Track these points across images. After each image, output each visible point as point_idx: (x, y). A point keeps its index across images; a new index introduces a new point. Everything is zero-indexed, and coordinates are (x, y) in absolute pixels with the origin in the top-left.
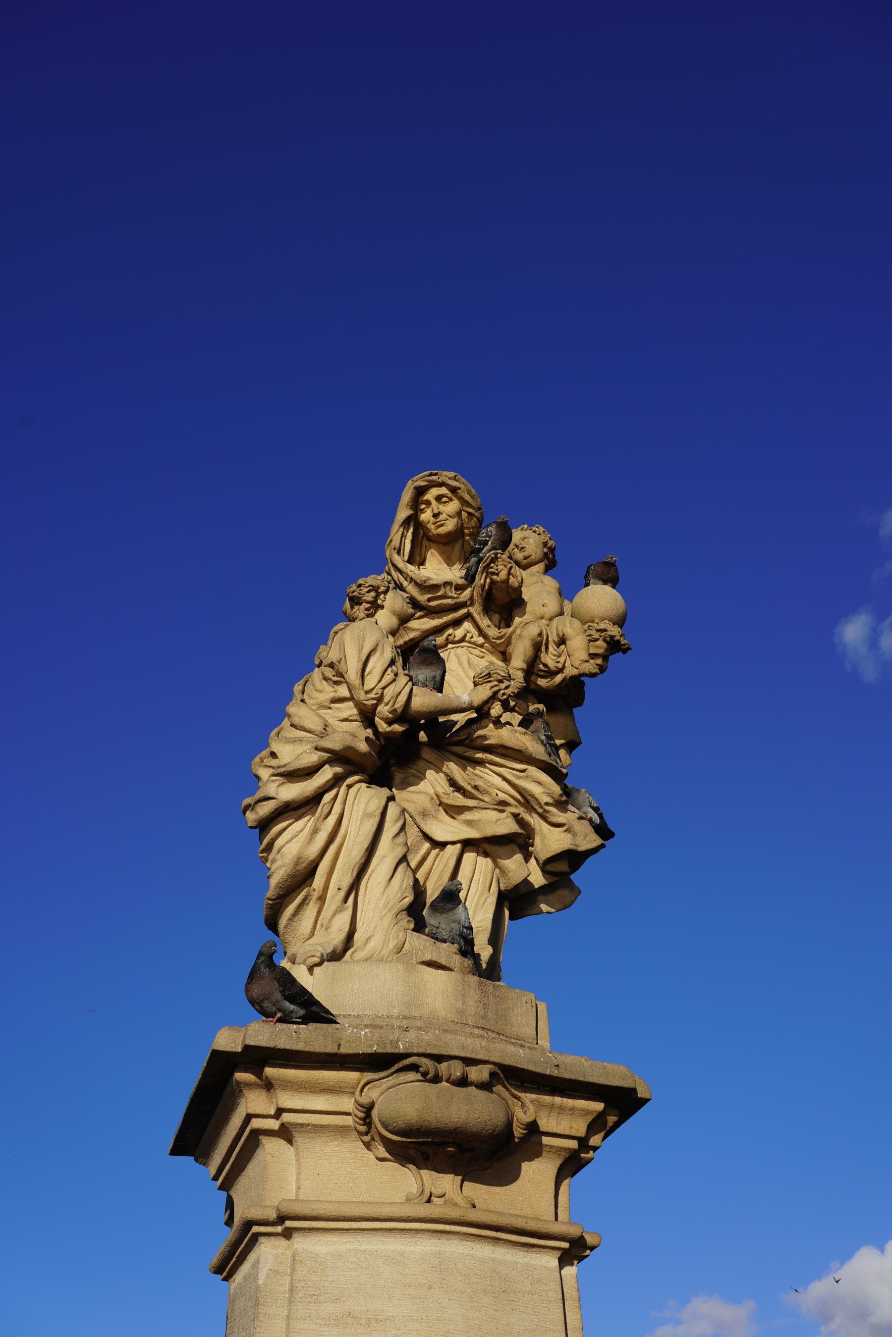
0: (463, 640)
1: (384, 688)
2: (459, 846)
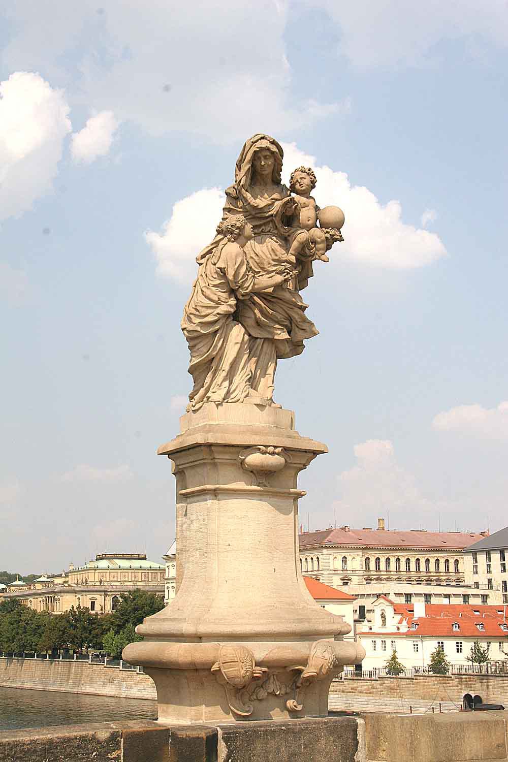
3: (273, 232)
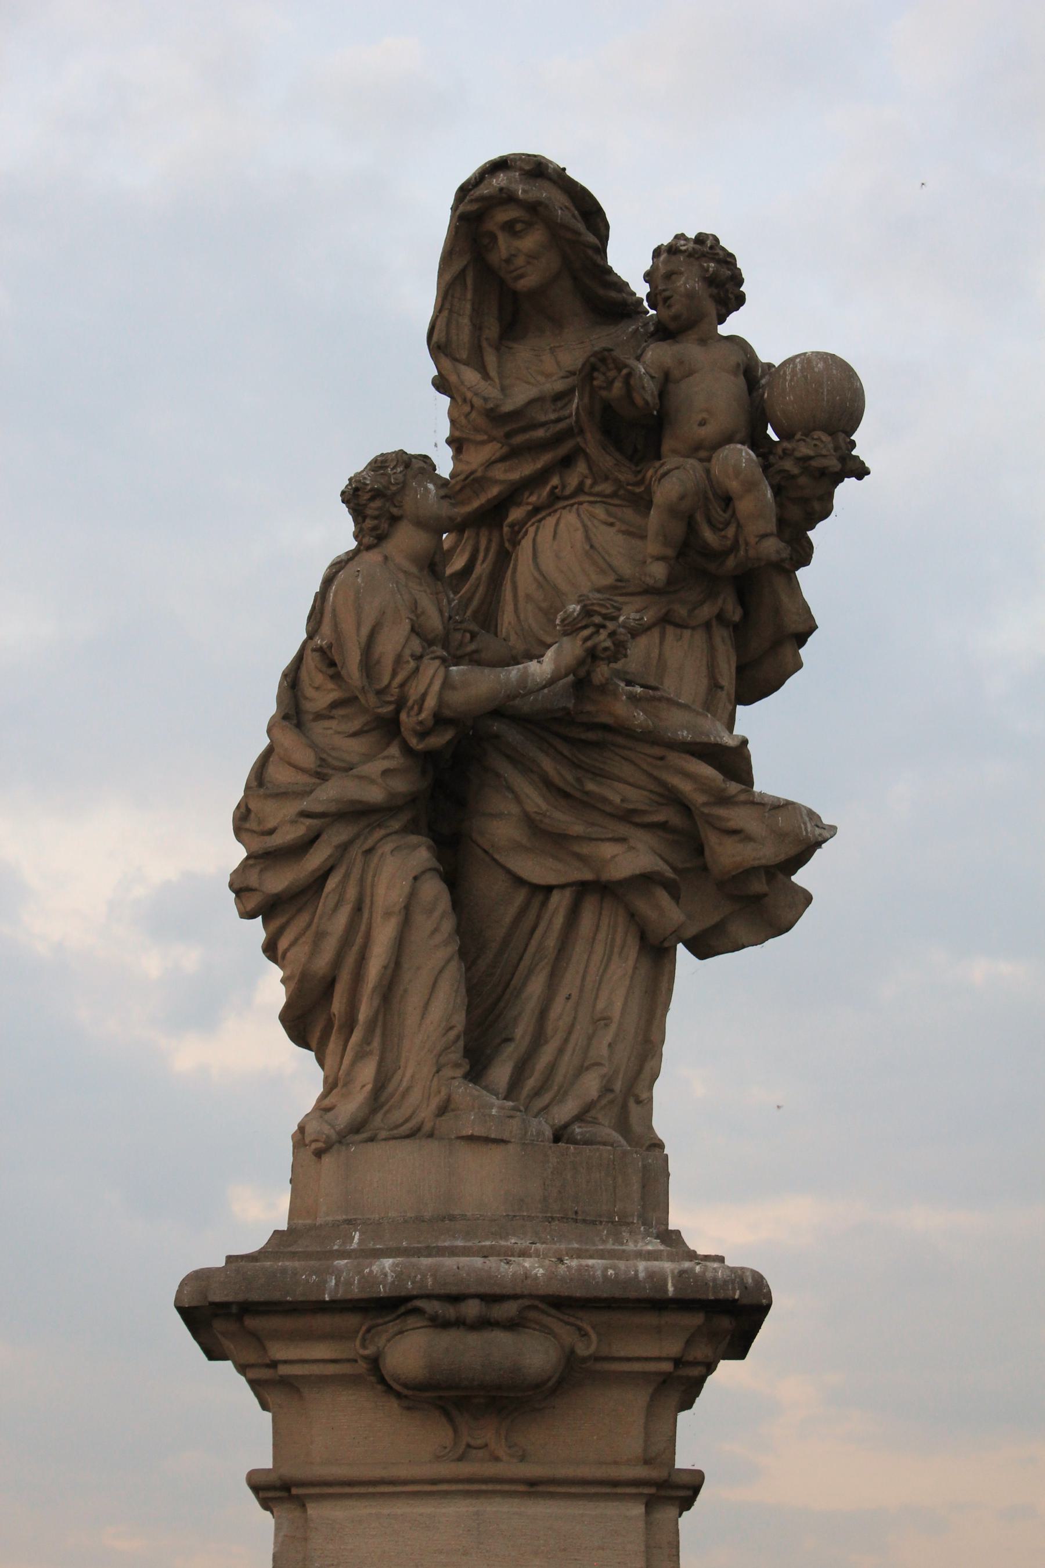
0: (580, 490)
1: (402, 685)
2: (568, 893)
3: (597, 489)
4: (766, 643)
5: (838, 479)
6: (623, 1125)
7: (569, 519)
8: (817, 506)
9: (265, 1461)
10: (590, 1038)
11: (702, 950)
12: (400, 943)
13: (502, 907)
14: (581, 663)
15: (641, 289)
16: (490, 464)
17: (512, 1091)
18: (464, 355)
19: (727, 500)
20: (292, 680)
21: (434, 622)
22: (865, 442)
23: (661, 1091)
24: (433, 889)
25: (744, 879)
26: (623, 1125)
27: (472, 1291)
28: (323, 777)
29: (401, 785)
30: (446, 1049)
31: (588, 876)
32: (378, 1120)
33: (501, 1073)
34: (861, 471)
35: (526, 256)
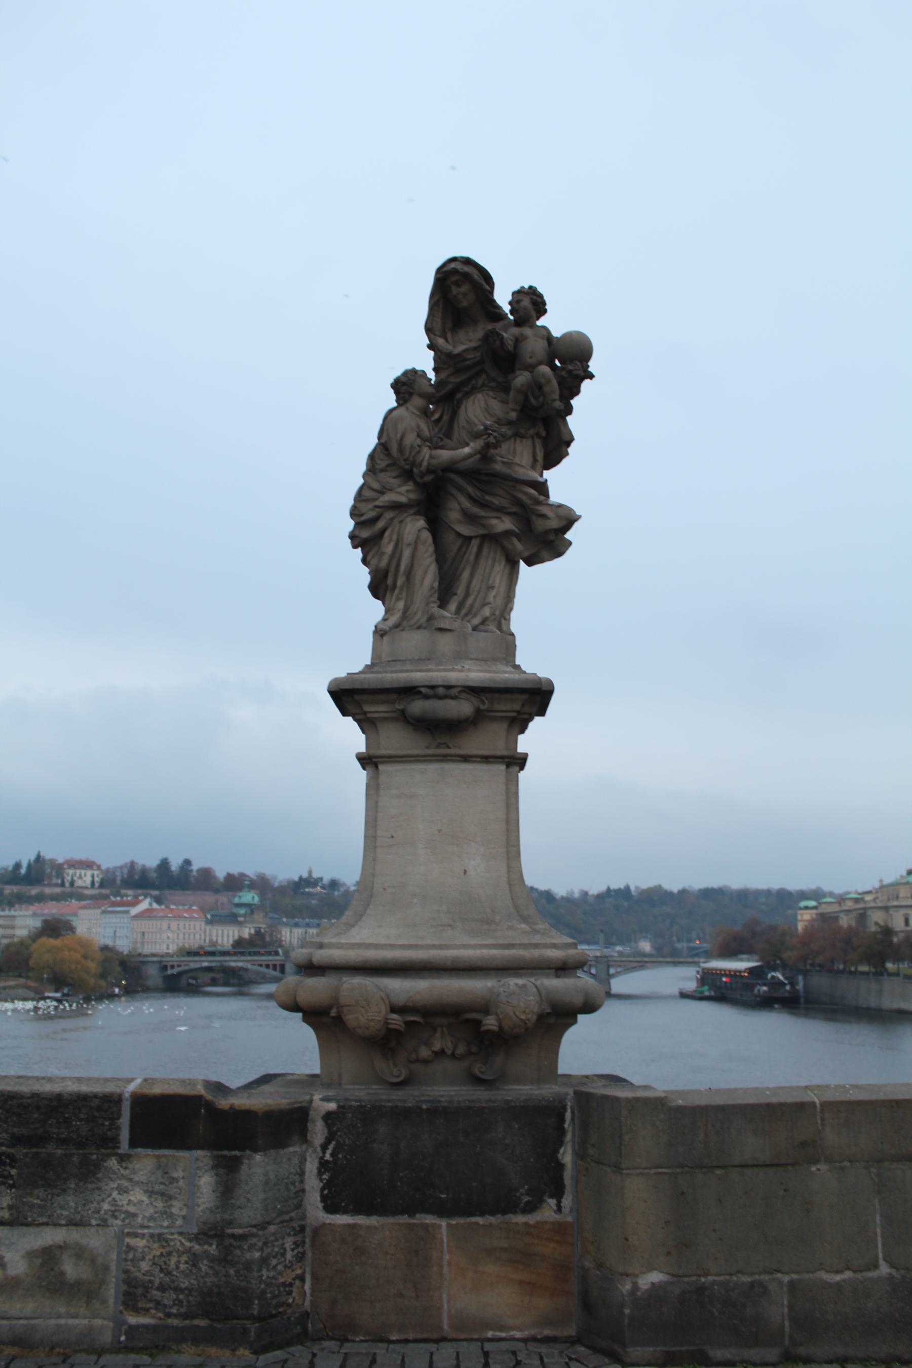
0: (483, 385)
4: (556, 447)
5: (582, 379)
6: (499, 628)
7: (480, 396)
8: (575, 390)
9: (363, 749)
10: (486, 594)
11: (530, 563)
12: (413, 557)
13: (453, 545)
14: (483, 448)
15: (507, 308)
16: (448, 376)
17: (458, 612)
18: (438, 333)
19: (540, 387)
20: (372, 457)
21: (426, 433)
22: (593, 366)
23: (513, 615)
24: (426, 535)
25: (545, 534)
26: (499, 628)
27: (440, 683)
28: (382, 493)
29: (413, 496)
30: (431, 596)
31: (484, 532)
32: (405, 623)
33: (453, 606)
34: (591, 376)
35: (463, 294)
